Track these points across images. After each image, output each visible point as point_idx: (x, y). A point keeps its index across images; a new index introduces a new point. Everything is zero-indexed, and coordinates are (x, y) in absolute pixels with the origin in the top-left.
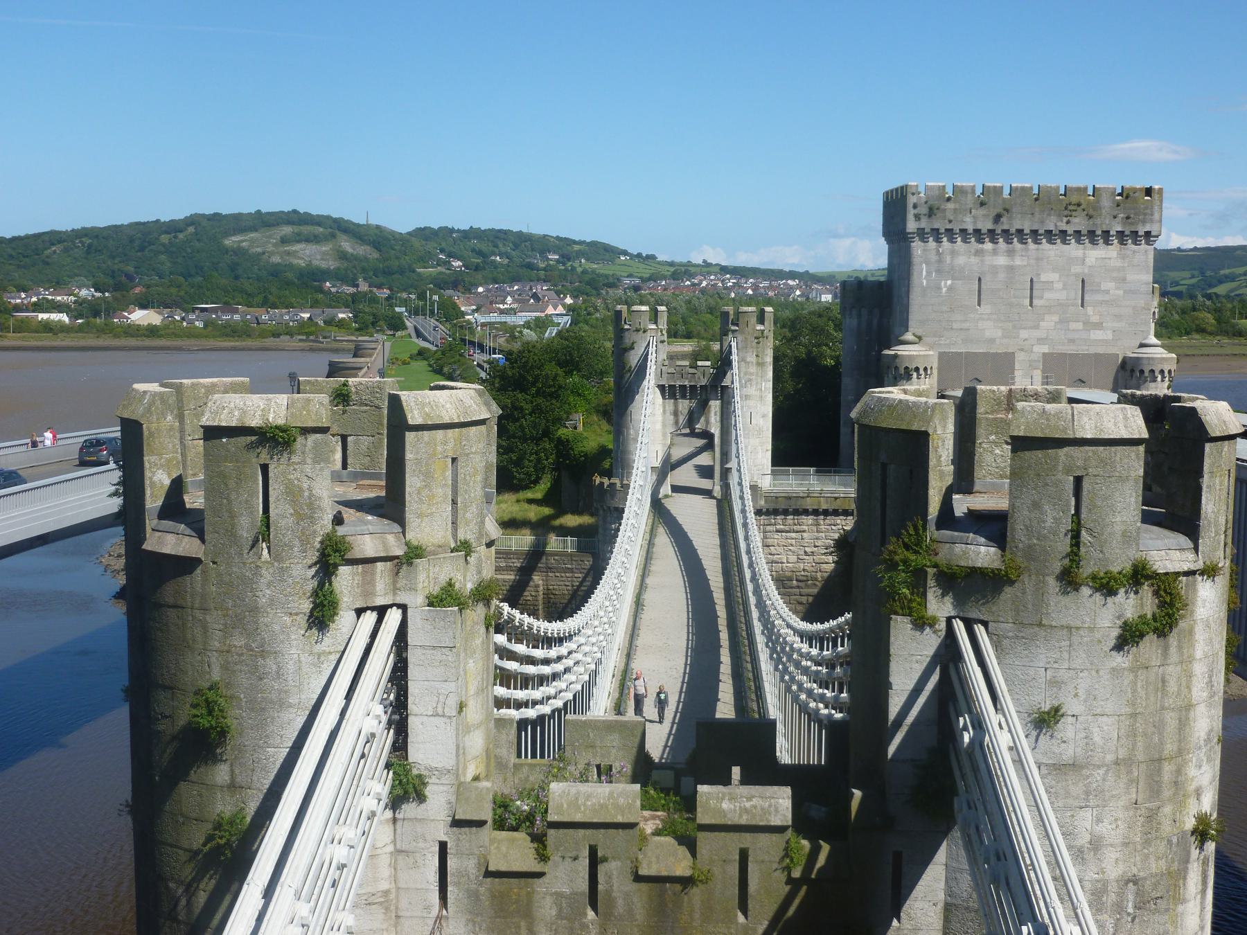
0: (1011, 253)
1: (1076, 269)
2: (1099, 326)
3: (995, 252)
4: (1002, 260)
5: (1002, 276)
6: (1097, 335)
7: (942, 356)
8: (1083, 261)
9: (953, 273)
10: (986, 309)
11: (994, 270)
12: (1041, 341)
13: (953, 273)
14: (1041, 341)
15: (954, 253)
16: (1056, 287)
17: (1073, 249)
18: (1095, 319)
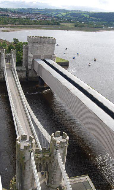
0: (41, 45)
1: (47, 47)
2: (49, 52)
3: (39, 45)
4: (40, 46)
5: (40, 47)
6: (49, 53)
7: (34, 55)
8: (48, 46)
9: (35, 47)
10: (38, 51)
11: (39, 47)
12: (44, 54)
13: (35, 47)
14: (44, 54)
15: (35, 45)
16: (45, 49)
17: (47, 45)
18: (49, 52)
